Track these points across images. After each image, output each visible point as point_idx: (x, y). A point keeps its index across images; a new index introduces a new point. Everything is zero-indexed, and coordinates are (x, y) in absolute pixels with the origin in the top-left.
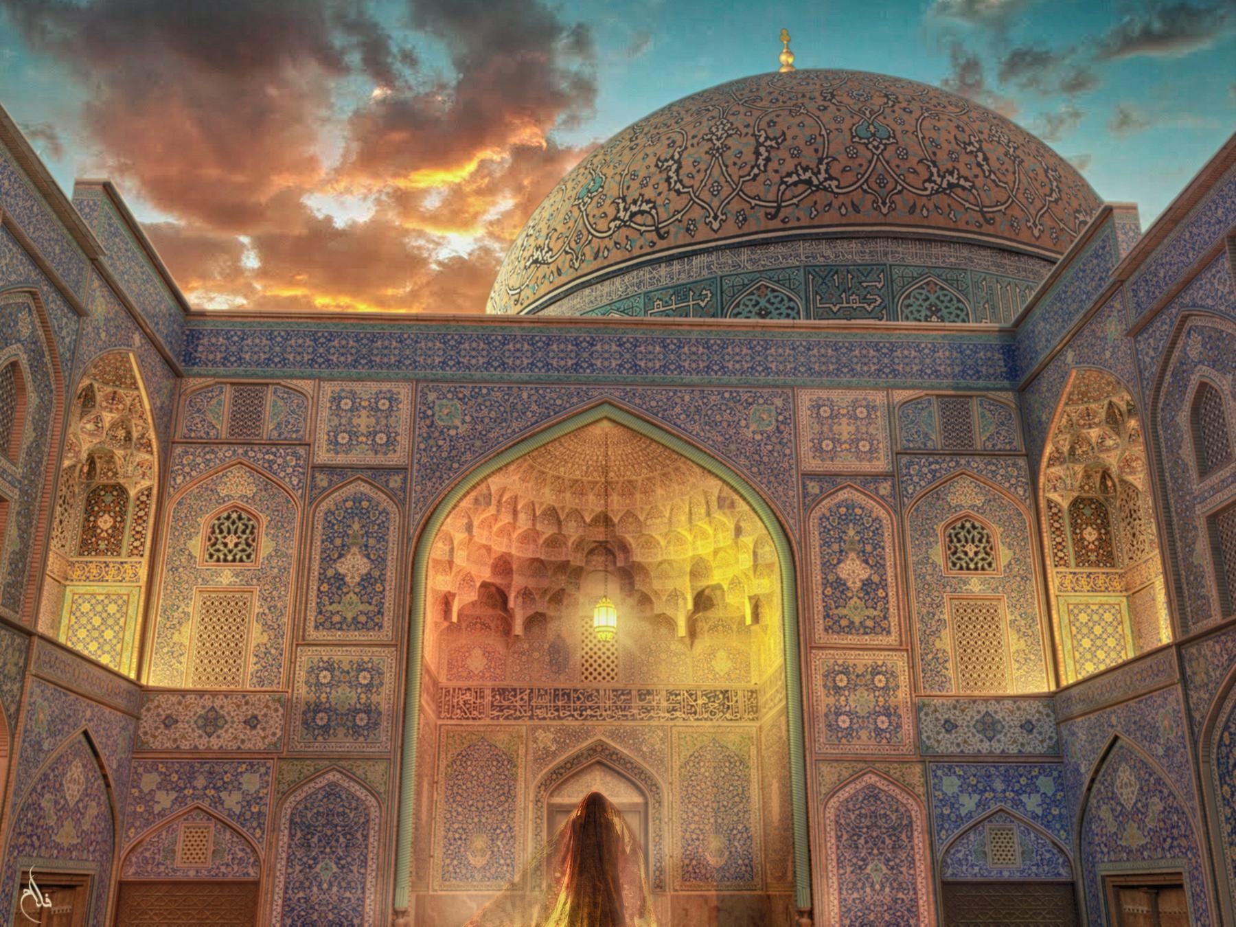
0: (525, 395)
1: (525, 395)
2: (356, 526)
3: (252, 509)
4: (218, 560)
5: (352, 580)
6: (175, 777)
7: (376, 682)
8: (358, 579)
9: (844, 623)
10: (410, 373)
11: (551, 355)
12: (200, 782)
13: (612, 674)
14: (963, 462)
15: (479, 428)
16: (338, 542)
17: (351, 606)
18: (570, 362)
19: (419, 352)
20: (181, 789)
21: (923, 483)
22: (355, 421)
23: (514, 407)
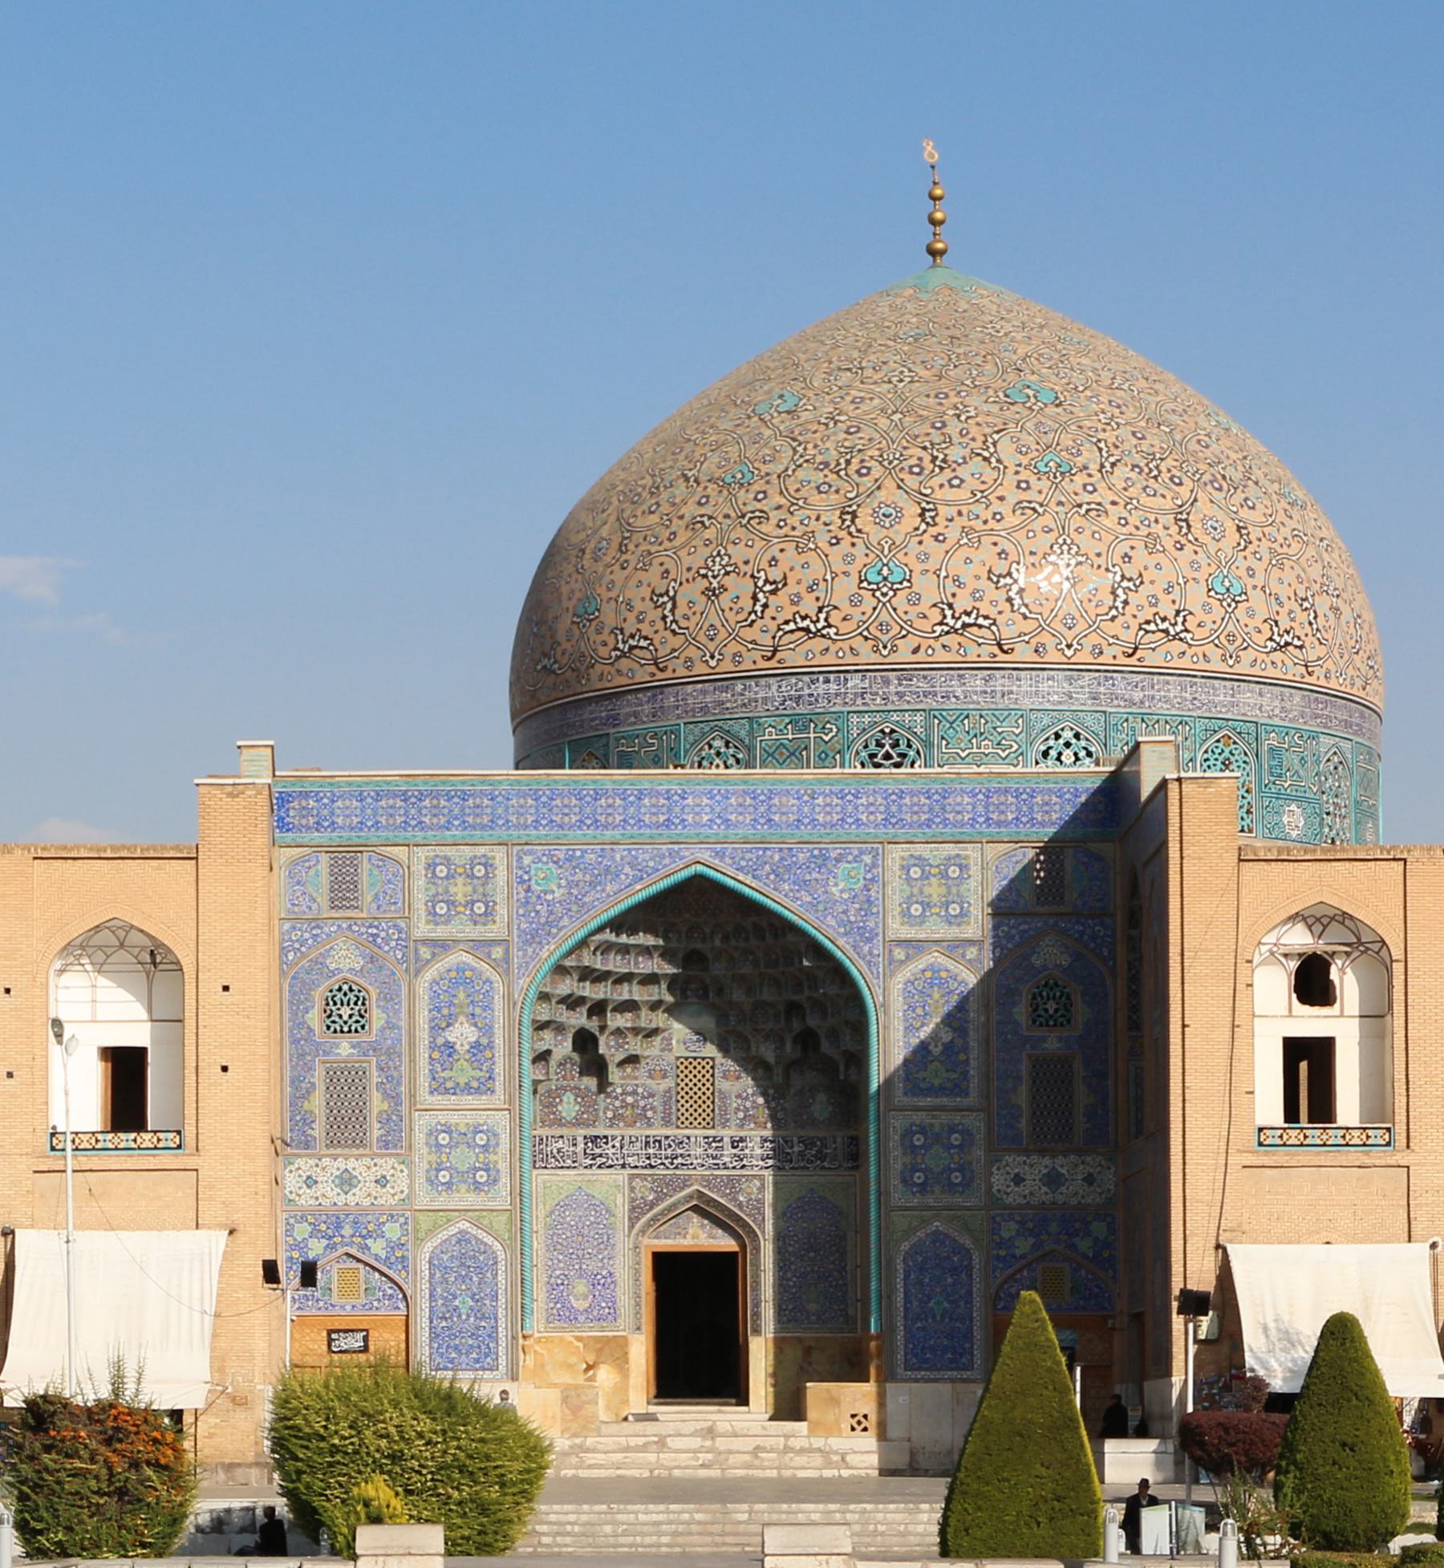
0: (618, 857)
1: (618, 857)
2: (462, 996)
3: (361, 982)
4: (335, 1031)
5: (462, 1048)
6: (323, 1227)
7: (492, 1142)
8: (467, 1047)
9: (923, 1085)
10: (502, 834)
11: (643, 810)
12: (347, 1231)
13: (708, 1119)
14: (1051, 921)
15: (575, 892)
16: (445, 1011)
17: (463, 1072)
18: (662, 818)
19: (511, 810)
20: (330, 1238)
21: (1010, 946)
22: (453, 890)
23: (607, 870)
